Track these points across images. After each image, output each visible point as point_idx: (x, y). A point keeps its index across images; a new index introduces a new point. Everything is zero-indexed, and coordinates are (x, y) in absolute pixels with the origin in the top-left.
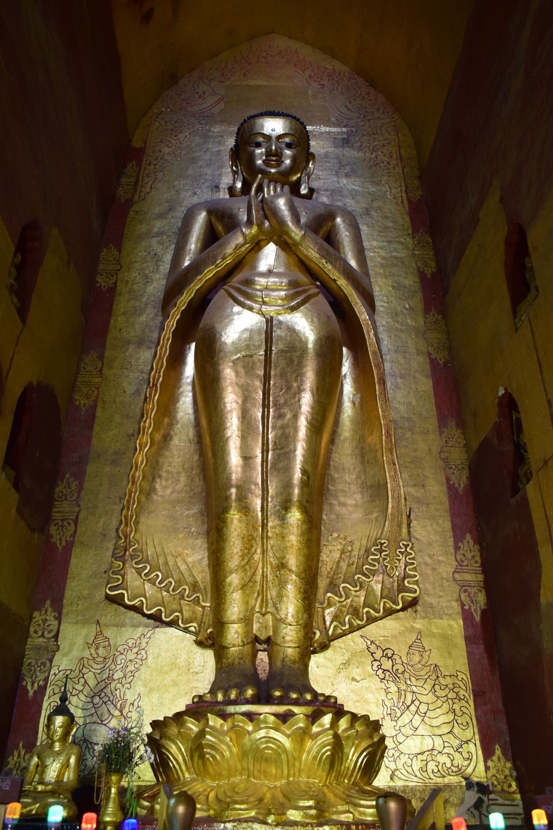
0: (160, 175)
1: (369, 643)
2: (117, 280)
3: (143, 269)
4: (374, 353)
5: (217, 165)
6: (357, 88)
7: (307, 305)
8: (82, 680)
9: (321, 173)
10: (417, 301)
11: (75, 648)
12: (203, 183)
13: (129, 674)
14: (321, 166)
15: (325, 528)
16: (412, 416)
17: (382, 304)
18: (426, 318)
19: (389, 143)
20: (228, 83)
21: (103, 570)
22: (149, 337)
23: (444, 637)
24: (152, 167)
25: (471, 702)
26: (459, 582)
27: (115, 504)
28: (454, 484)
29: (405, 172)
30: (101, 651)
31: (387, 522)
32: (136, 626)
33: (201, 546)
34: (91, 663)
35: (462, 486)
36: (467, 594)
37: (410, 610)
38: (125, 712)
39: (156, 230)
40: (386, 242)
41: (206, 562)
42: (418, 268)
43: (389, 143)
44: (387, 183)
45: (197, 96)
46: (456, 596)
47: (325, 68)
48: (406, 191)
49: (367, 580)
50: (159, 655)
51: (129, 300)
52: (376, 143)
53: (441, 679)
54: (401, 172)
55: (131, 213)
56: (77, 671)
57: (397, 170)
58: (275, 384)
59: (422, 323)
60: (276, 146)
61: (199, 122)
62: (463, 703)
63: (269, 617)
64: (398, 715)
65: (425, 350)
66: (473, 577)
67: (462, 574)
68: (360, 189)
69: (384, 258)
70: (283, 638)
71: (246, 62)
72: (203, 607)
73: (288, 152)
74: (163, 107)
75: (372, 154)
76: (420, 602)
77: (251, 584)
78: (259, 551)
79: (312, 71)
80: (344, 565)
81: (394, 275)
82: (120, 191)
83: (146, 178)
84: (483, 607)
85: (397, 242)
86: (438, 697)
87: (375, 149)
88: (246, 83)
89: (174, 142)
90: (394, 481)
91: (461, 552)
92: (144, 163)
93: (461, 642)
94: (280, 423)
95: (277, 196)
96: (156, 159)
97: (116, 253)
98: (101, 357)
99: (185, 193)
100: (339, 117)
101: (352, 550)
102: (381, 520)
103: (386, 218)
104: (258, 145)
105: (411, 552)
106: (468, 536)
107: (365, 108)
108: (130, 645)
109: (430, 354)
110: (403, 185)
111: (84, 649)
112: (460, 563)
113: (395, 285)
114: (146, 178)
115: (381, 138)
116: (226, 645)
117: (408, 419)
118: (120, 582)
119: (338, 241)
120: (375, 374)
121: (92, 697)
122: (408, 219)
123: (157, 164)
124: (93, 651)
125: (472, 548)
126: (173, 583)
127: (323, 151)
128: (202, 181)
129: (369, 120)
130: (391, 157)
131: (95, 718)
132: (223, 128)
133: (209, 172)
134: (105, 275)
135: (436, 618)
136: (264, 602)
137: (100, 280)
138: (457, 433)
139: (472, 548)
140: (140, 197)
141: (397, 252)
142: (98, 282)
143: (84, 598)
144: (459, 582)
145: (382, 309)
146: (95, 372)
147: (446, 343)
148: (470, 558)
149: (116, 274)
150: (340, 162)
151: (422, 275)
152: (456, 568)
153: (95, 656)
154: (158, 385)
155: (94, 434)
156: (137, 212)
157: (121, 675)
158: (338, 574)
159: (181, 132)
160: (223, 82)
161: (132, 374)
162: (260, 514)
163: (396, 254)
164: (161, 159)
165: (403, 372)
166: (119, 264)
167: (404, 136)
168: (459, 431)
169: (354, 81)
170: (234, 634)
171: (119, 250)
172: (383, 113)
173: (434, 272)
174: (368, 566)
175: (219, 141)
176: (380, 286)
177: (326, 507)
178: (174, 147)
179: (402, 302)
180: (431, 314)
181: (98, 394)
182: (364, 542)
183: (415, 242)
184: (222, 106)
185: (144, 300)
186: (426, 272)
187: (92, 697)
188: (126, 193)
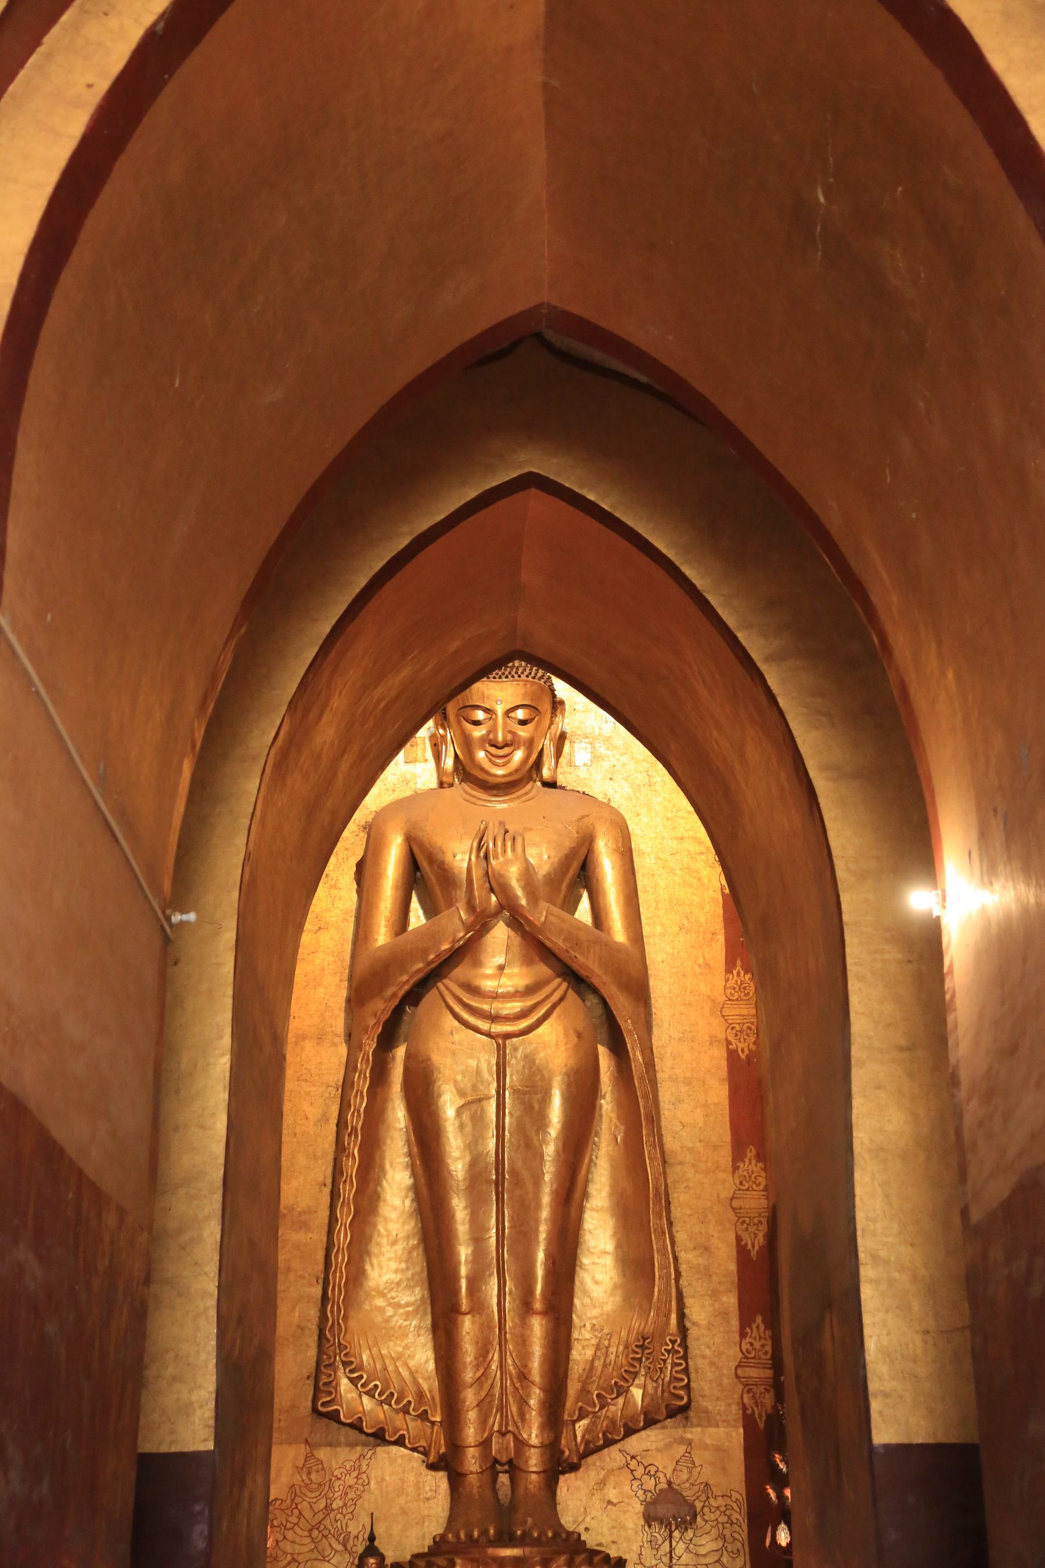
1: (629, 1458)
4: (641, 1078)
8: (296, 1512)
11: (283, 1473)
13: (350, 1503)
15: (578, 1317)
16: (698, 1144)
18: (727, 980)
21: (305, 1376)
23: (719, 1449)
25: (745, 1527)
27: (311, 1285)
28: (746, 1245)
30: (313, 1476)
32: (351, 1445)
33: (425, 1345)
34: (304, 1490)
35: (757, 1248)
37: (679, 1417)
38: (349, 1546)
40: (676, 838)
46: (736, 1397)
49: (626, 1385)
50: (383, 1479)
53: (712, 1500)
56: (289, 1501)
59: (721, 988)
60: (503, 735)
62: (736, 1528)
63: (510, 1437)
64: (660, 1542)
65: (722, 1036)
66: (759, 1373)
67: (747, 1369)
70: (527, 1462)
72: (433, 1423)
77: (488, 1399)
78: (496, 1357)
80: (599, 1364)
84: (769, 1411)
86: (706, 1521)
91: (748, 1340)
93: (739, 1454)
94: (518, 1192)
95: (508, 862)
102: (645, 1306)
104: (477, 723)
106: (759, 1319)
108: (348, 1468)
109: (728, 1043)
111: (293, 1475)
116: (463, 1471)
117: (691, 1150)
121: (310, 1531)
124: (304, 1477)
125: (762, 1335)
131: (315, 1555)
135: (710, 1426)
136: (504, 1418)
138: (756, 1168)
139: (762, 1335)
143: (287, 1411)
147: (752, 1023)
153: (308, 1482)
157: (341, 1504)
161: (314, 1089)
162: (495, 1309)
165: (688, 1074)
168: (760, 1165)
170: (472, 1461)
176: (663, 925)
182: (624, 1334)
185: (317, 962)
187: (310, 1531)
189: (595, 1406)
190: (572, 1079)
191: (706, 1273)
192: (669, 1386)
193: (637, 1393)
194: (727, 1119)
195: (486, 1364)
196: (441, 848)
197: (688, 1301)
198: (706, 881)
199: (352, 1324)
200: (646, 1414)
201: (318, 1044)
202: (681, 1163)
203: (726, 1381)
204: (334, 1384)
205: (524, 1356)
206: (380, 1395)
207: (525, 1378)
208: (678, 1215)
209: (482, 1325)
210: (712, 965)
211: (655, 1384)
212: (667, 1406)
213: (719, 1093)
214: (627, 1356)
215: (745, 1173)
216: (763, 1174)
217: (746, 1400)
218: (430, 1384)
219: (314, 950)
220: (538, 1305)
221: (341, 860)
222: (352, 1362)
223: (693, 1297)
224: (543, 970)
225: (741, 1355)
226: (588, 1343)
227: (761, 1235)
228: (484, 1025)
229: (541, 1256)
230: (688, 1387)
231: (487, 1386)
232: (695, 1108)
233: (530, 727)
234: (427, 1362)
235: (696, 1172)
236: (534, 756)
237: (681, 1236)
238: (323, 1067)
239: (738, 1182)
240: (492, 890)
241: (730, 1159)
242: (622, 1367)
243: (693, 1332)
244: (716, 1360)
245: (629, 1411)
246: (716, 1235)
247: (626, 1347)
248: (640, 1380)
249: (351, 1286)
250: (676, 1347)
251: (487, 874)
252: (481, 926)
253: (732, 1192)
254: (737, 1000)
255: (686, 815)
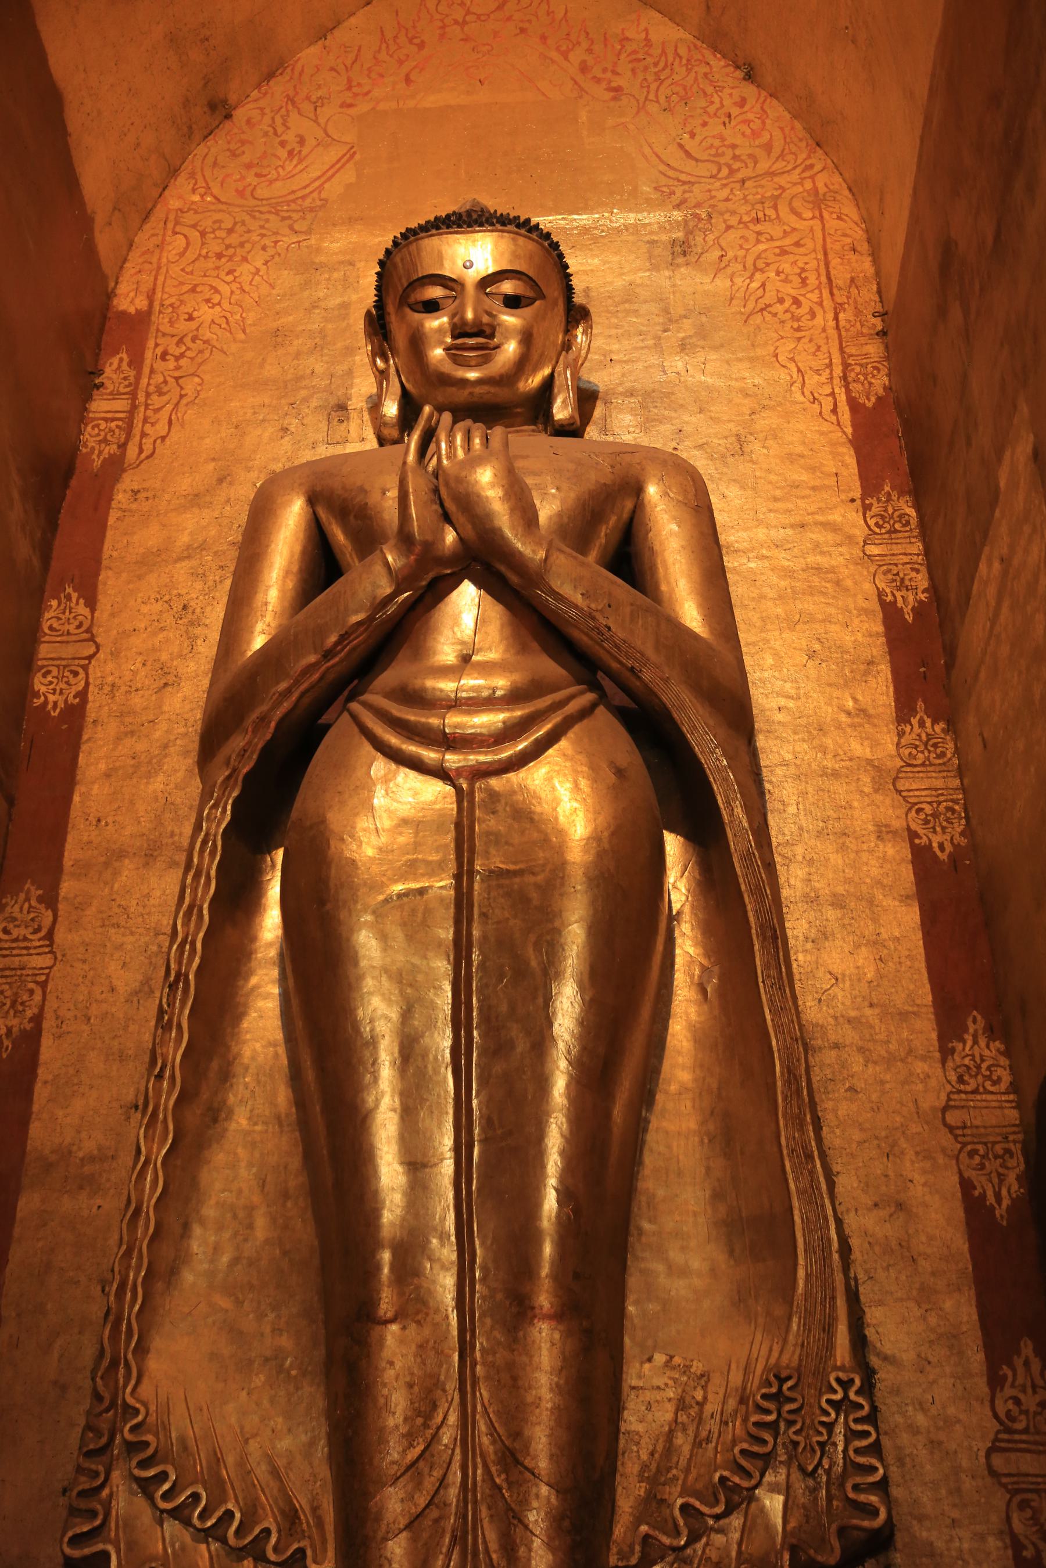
0: (190, 386)
2: (87, 684)
3: (154, 649)
4: (747, 857)
5: (339, 345)
6: (710, 90)
7: (563, 744)
9: (616, 347)
10: (879, 691)
12: (305, 400)
14: (617, 327)
16: (868, 1012)
17: (783, 702)
18: (901, 734)
19: (797, 244)
20: (363, 107)
22: (172, 834)
24: (171, 364)
26: (1004, 1480)
28: (983, 1196)
29: (842, 323)
31: (795, 1320)
35: (1006, 1202)
36: (1029, 1513)
39: (185, 538)
40: (792, 526)
41: (321, 1450)
42: (880, 594)
43: (797, 244)
44: (792, 359)
45: (283, 153)
47: (624, 40)
48: (845, 378)
51: (118, 739)
52: (762, 247)
54: (832, 323)
55: (121, 497)
57: (819, 320)
58: (482, 965)
59: (891, 748)
60: (475, 311)
61: (291, 227)
65: (898, 824)
67: (1013, 1456)
68: (720, 383)
69: (788, 573)
71: (411, 41)
73: (510, 319)
74: (194, 191)
75: (751, 278)
76: (900, 1539)
77: (434, 1513)
78: (453, 1419)
79: (590, 51)
81: (811, 619)
82: (90, 437)
83: (155, 397)
85: (822, 524)
87: (760, 264)
88: (411, 103)
89: (225, 289)
90: (810, 1203)
91: (1008, 1391)
92: (149, 355)
94: (498, 1068)
95: (473, 462)
96: (180, 341)
97: (82, 610)
98: (51, 900)
99: (259, 431)
100: (663, 181)
101: (705, 1398)
103: (792, 458)
104: (432, 307)
105: (861, 1400)
106: (1027, 1348)
107: (734, 146)
109: (913, 835)
110: (837, 360)
112: (1005, 1424)
113: (817, 647)
114: (155, 397)
115: (776, 231)
118: (98, 1522)
119: (651, 549)
120: (751, 915)
122: (851, 460)
123: (182, 355)
126: (238, 1515)
127: (619, 283)
128: (303, 393)
129: (743, 182)
130: (804, 281)
132: (354, 238)
133: (319, 368)
134: (55, 672)
137: (43, 689)
138: (990, 1051)
140: (141, 451)
141: (822, 553)
142: (37, 695)
144: (1004, 1480)
145: (779, 717)
146: (36, 940)
147: (955, 802)
148: (1033, 1408)
149: (85, 668)
150: (666, 311)
151: (890, 612)
152: (996, 1439)
154: (191, 977)
155: (35, 1108)
156: (135, 493)
158: (669, 1469)
159: (245, 259)
160: (350, 106)
161: (131, 939)
163: (819, 559)
164: (193, 340)
165: (840, 889)
166: (92, 639)
167: (839, 218)
169: (704, 69)
171: (92, 603)
172: (782, 156)
173: (921, 602)
174: (745, 1446)
175: (345, 279)
176: (776, 654)
177: (633, 1281)
178: (225, 304)
179: (836, 693)
180: (915, 721)
181: (44, 999)
183: (871, 522)
184: (348, 175)
185: (157, 735)
186: (900, 603)
188: (105, 441)
189: (678, 1534)
190: (607, 846)
191: (903, 1252)
192: (842, 1485)
193: (774, 1504)
194: (922, 965)
195: (429, 1433)
196: (362, 490)
197: (873, 1315)
198: (849, 583)
199: (153, 1364)
200: (794, 1550)
201: (146, 864)
202: (836, 1046)
203: (968, 1484)
204: (105, 1493)
205: (514, 1414)
206: (203, 1516)
207: (518, 1462)
208: (837, 1142)
209: (421, 1347)
210: (872, 711)
211: (811, 1483)
212: (842, 1531)
213: (903, 921)
214: (745, 1420)
215: (967, 1061)
216: (1004, 1061)
217: (1017, 1525)
218: (312, 1485)
219: (151, 718)
220: (544, 1300)
221: (211, 583)
222: (147, 1444)
223: (880, 1303)
224: (550, 668)
225: (997, 1426)
226: (658, 1395)
227: (1012, 1177)
228: (430, 755)
229: (550, 1202)
230: (883, 1486)
231: (429, 1483)
232: (858, 946)
233: (527, 312)
234: (312, 1443)
235: (867, 1061)
236: (535, 381)
237: (845, 1183)
238: (152, 901)
239: (953, 1078)
240: (447, 518)
241: (934, 1035)
242: (734, 1443)
243: (885, 1376)
244: (942, 1436)
245: (755, 1547)
246: (917, 1177)
247: (743, 1401)
248: (775, 1476)
249: (160, 1286)
250: (852, 1396)
251: (436, 491)
252: (429, 591)
253: (943, 1097)
254: (923, 765)
255: (808, 492)
